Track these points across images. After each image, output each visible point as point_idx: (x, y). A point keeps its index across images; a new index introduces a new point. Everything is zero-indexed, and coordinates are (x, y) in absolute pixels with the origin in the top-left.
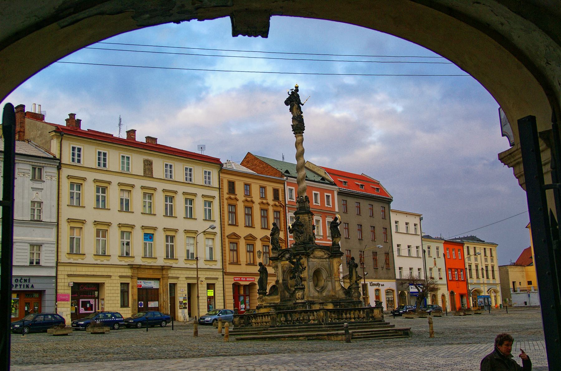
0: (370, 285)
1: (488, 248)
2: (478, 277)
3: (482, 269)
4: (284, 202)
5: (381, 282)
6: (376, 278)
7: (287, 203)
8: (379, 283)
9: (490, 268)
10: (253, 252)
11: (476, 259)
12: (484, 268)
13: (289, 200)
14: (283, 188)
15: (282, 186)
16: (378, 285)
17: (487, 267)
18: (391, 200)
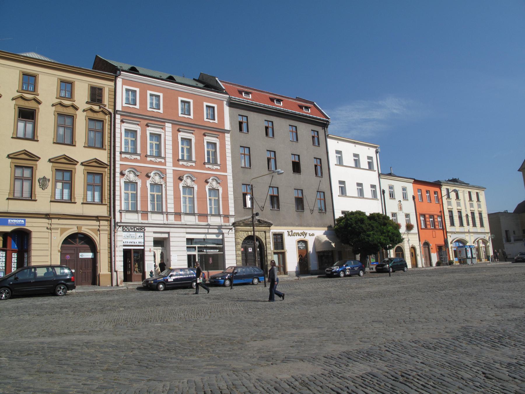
0: (289, 235)
1: (474, 192)
2: (462, 224)
3: (467, 216)
4: (113, 107)
5: (309, 231)
6: (301, 225)
7: (119, 108)
8: (306, 231)
9: (477, 215)
10: (31, 179)
11: (459, 204)
12: (470, 215)
13: (124, 105)
14: (113, 87)
15: (112, 84)
16: (304, 234)
17: (473, 213)
18: (328, 121)
